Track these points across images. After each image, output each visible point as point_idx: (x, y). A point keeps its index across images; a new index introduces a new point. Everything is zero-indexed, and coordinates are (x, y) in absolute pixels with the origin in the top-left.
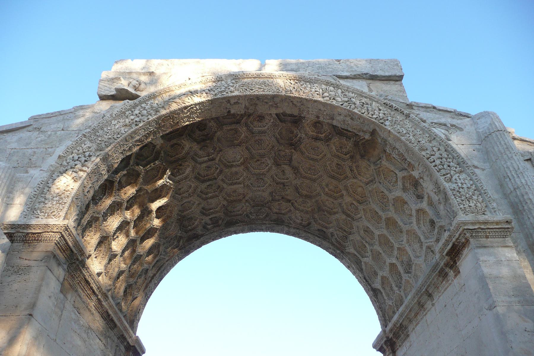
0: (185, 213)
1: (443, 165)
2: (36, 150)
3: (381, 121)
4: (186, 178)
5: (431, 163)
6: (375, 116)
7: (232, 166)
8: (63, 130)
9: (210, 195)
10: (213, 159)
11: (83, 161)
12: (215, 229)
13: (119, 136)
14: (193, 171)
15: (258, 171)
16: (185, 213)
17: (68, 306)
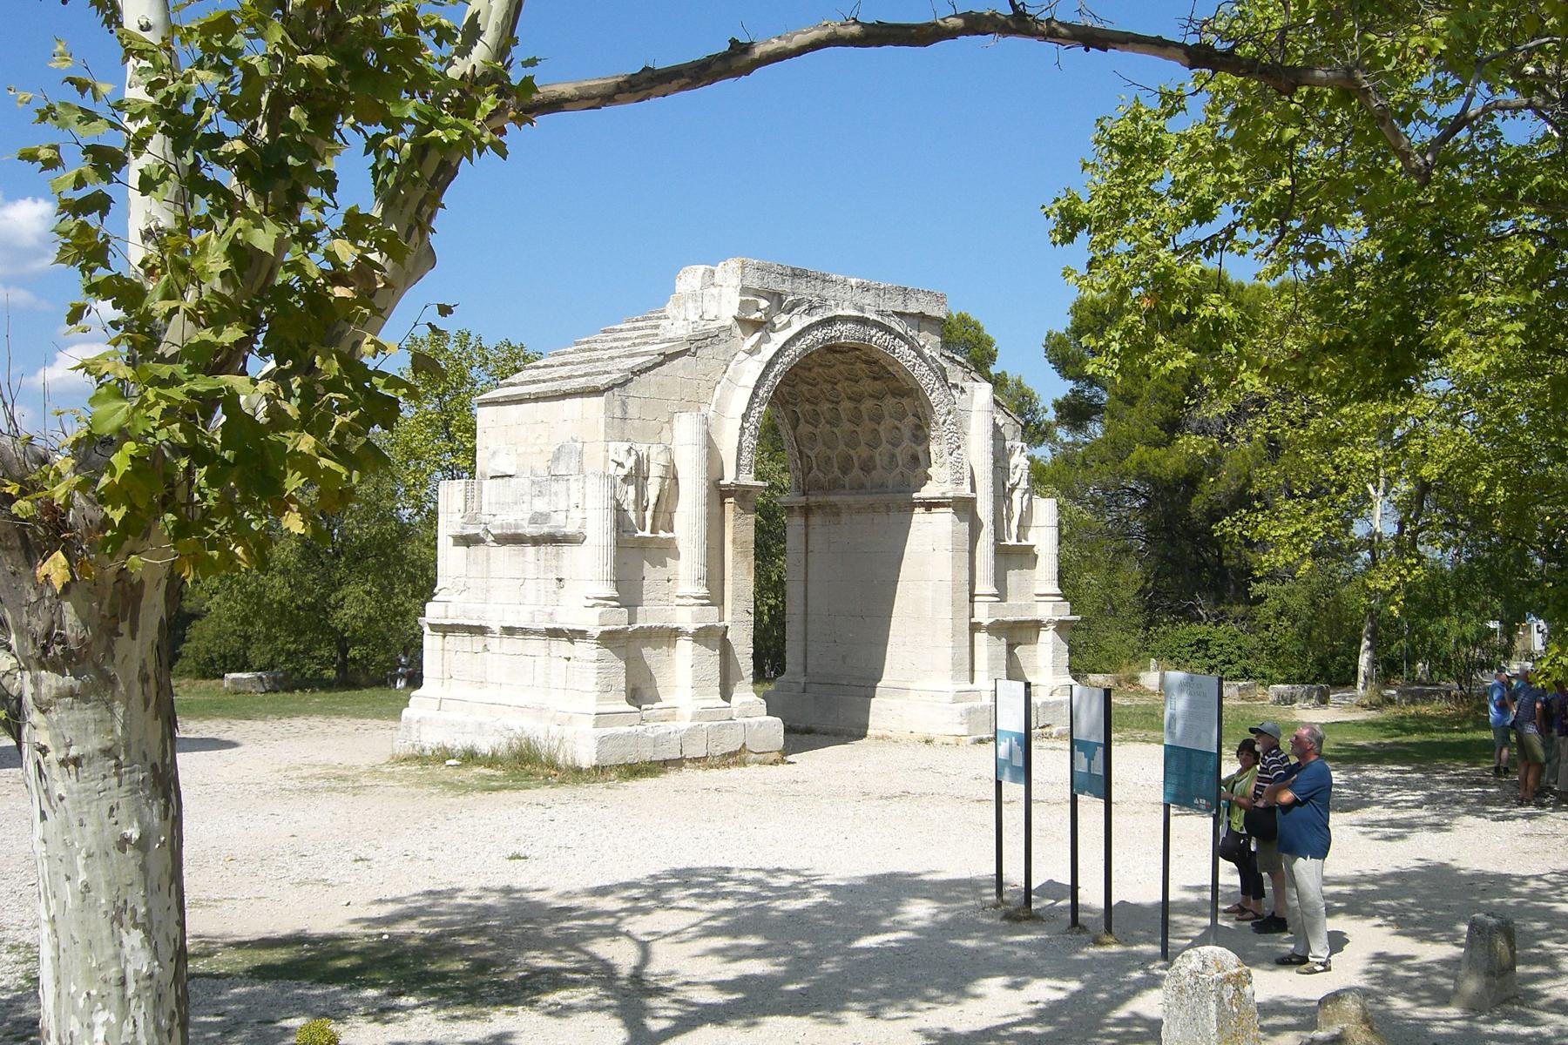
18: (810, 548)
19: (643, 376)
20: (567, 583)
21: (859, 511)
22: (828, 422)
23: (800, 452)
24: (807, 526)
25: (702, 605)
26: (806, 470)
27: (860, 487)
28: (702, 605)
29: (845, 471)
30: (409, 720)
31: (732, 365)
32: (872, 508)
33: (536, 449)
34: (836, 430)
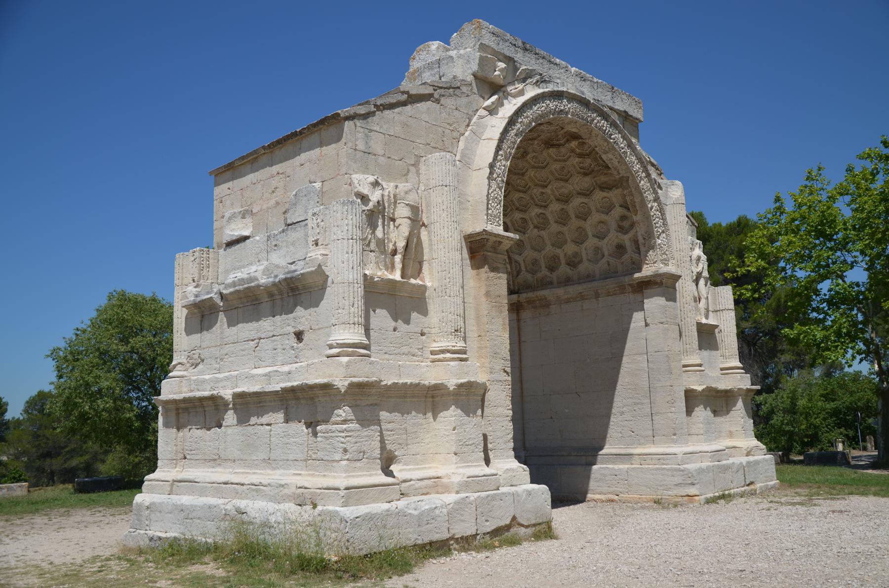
8: (456, 109)
18: (523, 339)
19: (387, 112)
20: (306, 337)
21: (568, 301)
22: (535, 227)
23: (509, 258)
24: (518, 320)
26: (515, 273)
27: (567, 281)
29: (552, 269)
30: (140, 506)
31: (475, 119)
32: (582, 297)
33: (272, 202)
34: (543, 233)
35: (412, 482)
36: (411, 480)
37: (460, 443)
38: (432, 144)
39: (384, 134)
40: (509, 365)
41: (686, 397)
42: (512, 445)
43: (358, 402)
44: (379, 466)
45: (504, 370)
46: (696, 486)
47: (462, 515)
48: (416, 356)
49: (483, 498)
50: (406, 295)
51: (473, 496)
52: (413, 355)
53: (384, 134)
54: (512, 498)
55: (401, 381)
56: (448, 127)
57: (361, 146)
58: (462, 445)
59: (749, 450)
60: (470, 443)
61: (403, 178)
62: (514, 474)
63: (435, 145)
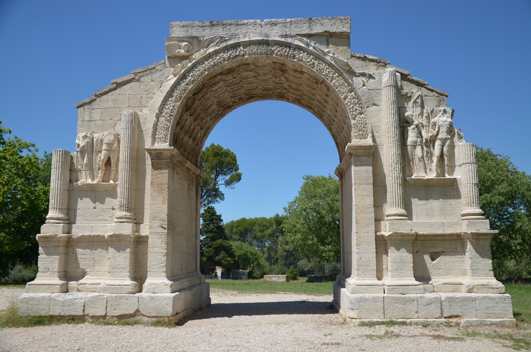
0: (221, 99)
1: (353, 109)
2: (142, 95)
3: (326, 77)
4: (220, 88)
5: (348, 107)
6: (324, 74)
7: (248, 78)
8: (152, 81)
9: (235, 89)
10: (235, 78)
11: (171, 109)
12: (240, 102)
13: (185, 91)
14: (224, 84)
15: (264, 78)
16: (221, 99)
17: (175, 174)
25: (121, 222)
28: (121, 222)
35: (86, 285)
36: (85, 284)
37: (112, 267)
38: (133, 106)
39: (101, 109)
40: (166, 224)
41: (376, 240)
42: (165, 269)
43: (47, 245)
44: (57, 276)
45: (161, 226)
46: (355, 311)
47: (96, 304)
48: (108, 221)
49: (113, 297)
50: (103, 190)
51: (106, 295)
52: (106, 220)
53: (101, 109)
54: (137, 299)
55: (92, 234)
56: (145, 92)
57: (87, 118)
58: (113, 268)
59: (470, 287)
60: (119, 267)
61: (112, 129)
62: (156, 287)
63: (135, 106)
